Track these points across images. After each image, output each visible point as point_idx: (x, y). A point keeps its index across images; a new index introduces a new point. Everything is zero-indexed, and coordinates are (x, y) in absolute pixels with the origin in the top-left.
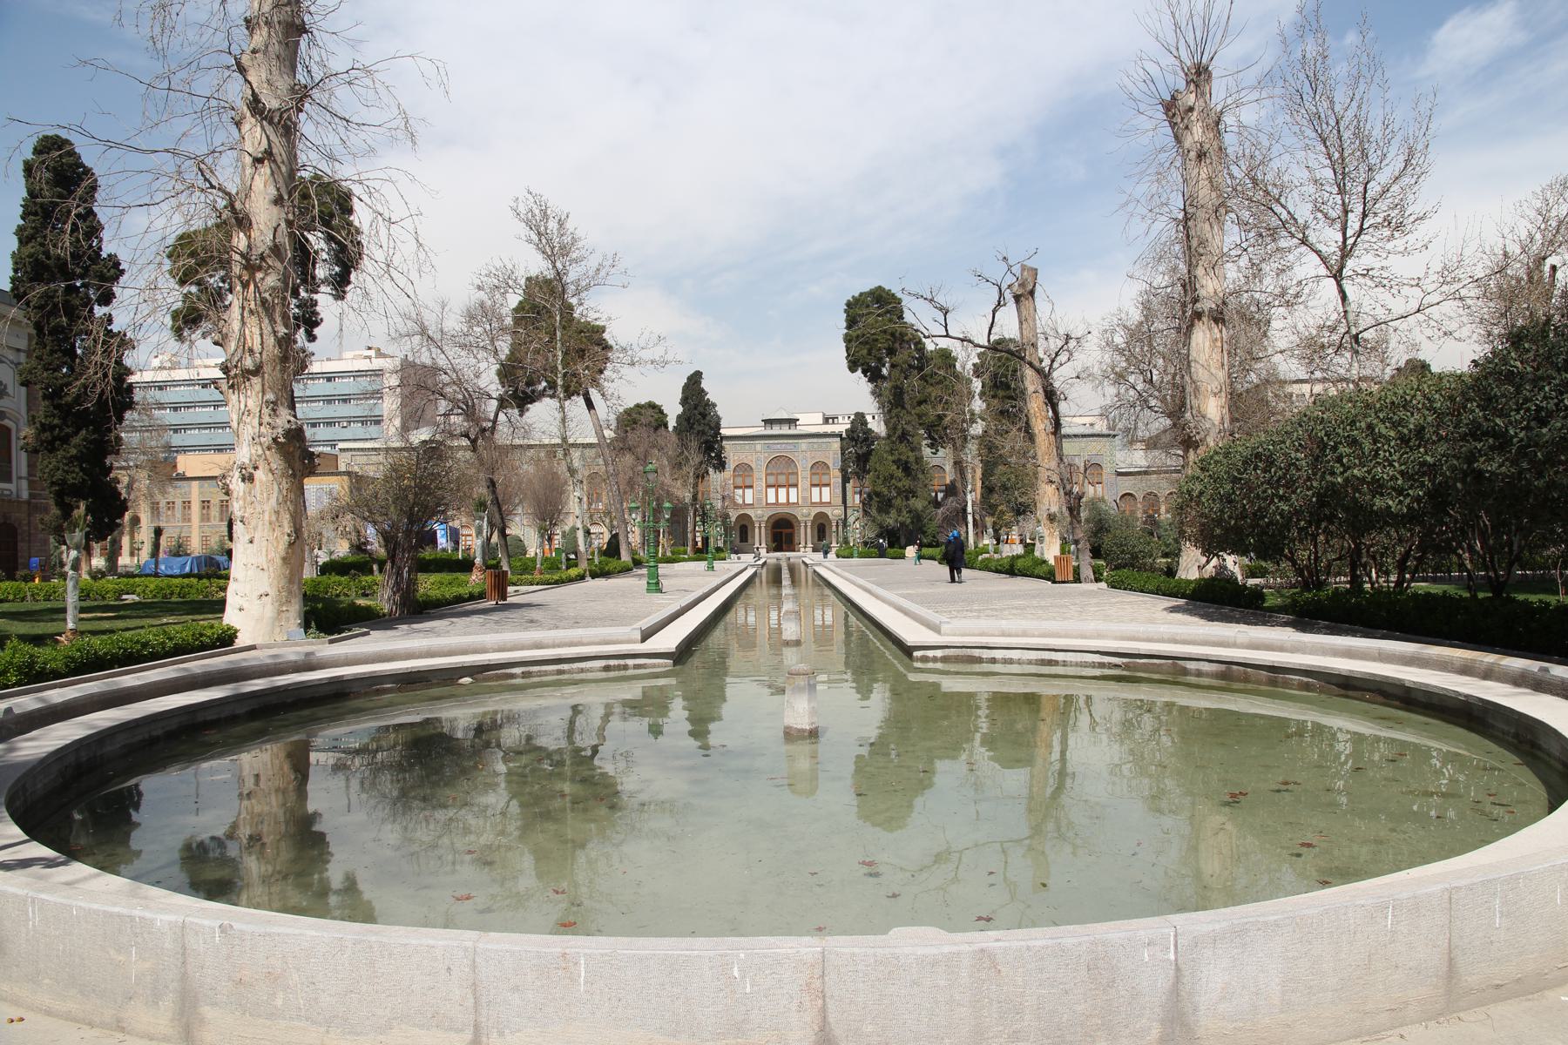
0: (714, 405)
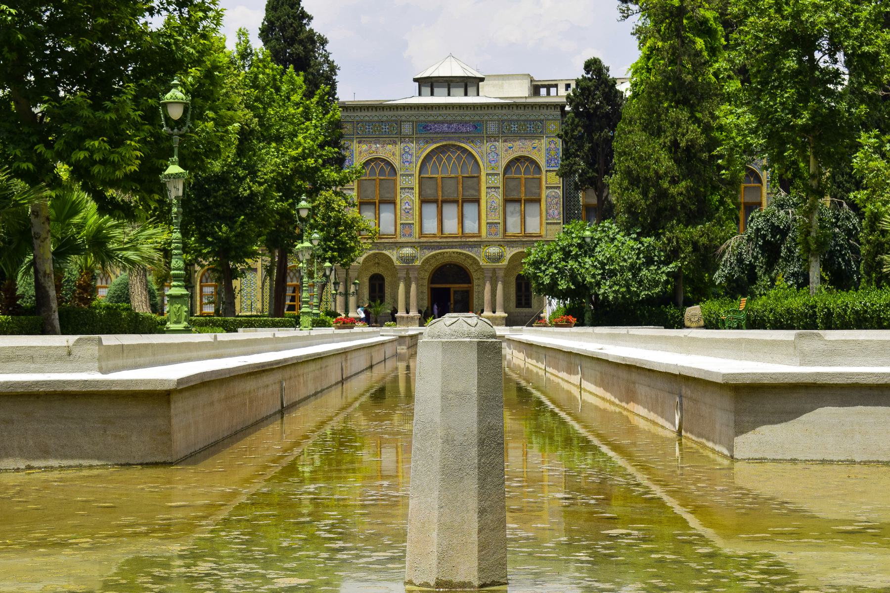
0: (324, 42)
